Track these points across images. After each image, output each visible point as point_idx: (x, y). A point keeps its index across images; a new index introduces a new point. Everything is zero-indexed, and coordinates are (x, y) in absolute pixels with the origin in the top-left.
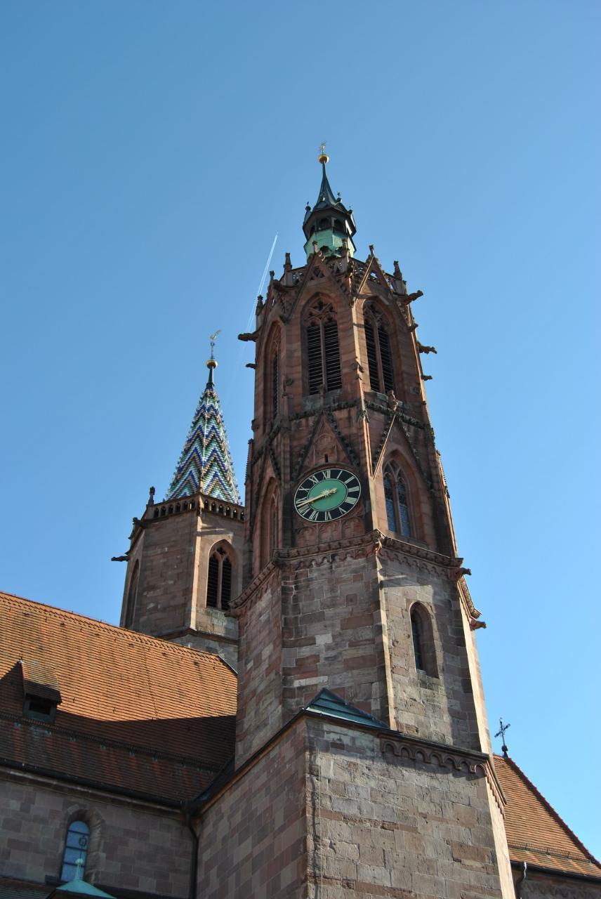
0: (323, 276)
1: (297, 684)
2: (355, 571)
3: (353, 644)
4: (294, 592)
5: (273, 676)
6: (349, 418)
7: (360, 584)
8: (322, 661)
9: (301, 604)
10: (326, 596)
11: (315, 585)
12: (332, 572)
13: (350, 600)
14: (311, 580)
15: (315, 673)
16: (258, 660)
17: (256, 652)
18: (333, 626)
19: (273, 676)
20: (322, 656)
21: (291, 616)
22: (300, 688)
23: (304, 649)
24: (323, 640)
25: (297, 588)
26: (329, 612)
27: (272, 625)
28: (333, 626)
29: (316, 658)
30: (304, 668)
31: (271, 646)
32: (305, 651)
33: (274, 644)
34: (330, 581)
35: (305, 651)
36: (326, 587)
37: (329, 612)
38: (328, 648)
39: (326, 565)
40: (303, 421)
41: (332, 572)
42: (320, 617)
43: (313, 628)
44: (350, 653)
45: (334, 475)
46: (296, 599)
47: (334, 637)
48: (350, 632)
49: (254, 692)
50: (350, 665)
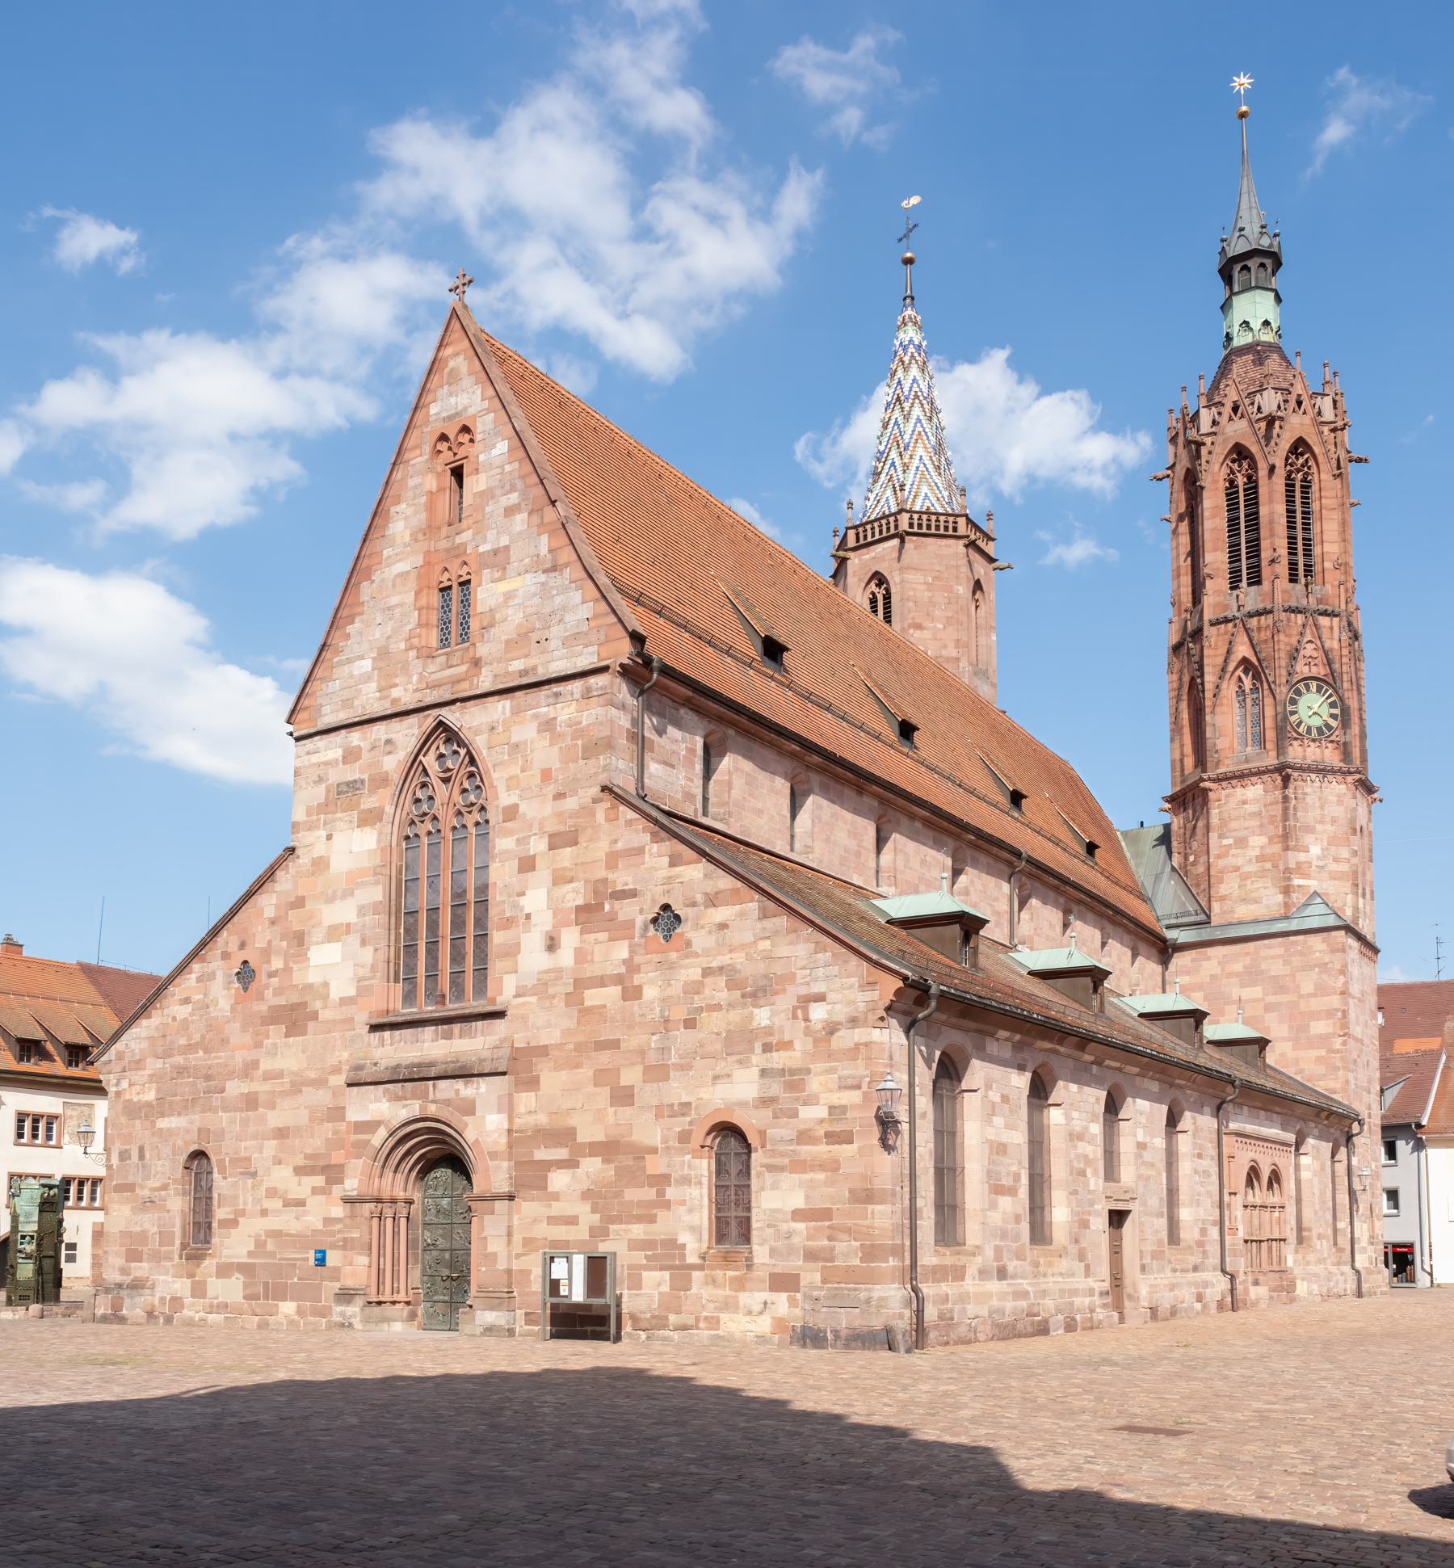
0: (1305, 413)
1: (1296, 882)
2: (1339, 796)
3: (1336, 860)
4: (1294, 802)
5: (1268, 865)
6: (1331, 628)
7: (1342, 809)
8: (1314, 868)
9: (1299, 814)
10: (1318, 812)
11: (1309, 800)
12: (1322, 792)
13: (1334, 821)
14: (1305, 794)
15: (1307, 876)
16: (1241, 843)
17: (1240, 834)
18: (1322, 840)
19: (1268, 865)
20: (1315, 863)
21: (1292, 823)
22: (1299, 886)
23: (1302, 854)
24: (1315, 850)
25: (1296, 798)
26: (1319, 827)
27: (1266, 821)
28: (1322, 840)
29: (1310, 863)
30: (1301, 869)
31: (1264, 840)
32: (1302, 857)
33: (1271, 839)
34: (1320, 799)
35: (1302, 857)
36: (1317, 804)
37: (1319, 827)
38: (1318, 858)
39: (1317, 784)
40: (1293, 615)
41: (1322, 792)
42: (1310, 829)
43: (1308, 839)
44: (1333, 867)
45: (1319, 690)
46: (1295, 809)
47: (1322, 849)
48: (1333, 848)
49: (1237, 869)
50: (1334, 876)
